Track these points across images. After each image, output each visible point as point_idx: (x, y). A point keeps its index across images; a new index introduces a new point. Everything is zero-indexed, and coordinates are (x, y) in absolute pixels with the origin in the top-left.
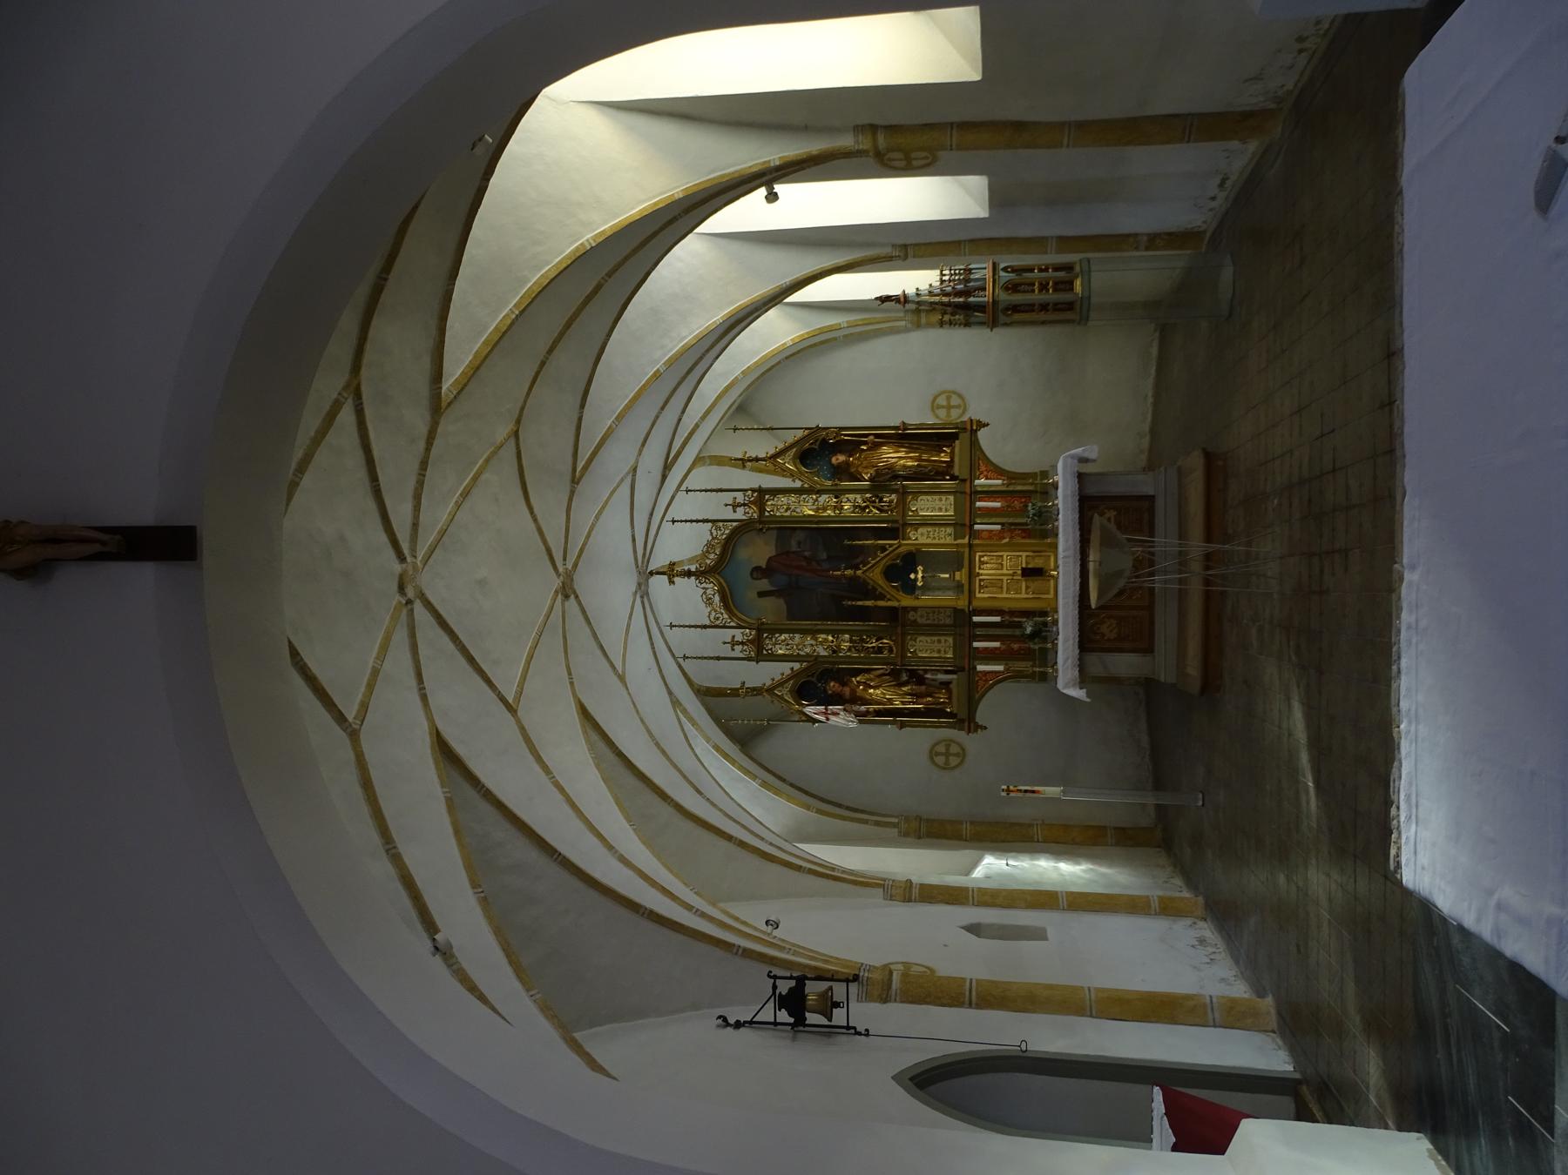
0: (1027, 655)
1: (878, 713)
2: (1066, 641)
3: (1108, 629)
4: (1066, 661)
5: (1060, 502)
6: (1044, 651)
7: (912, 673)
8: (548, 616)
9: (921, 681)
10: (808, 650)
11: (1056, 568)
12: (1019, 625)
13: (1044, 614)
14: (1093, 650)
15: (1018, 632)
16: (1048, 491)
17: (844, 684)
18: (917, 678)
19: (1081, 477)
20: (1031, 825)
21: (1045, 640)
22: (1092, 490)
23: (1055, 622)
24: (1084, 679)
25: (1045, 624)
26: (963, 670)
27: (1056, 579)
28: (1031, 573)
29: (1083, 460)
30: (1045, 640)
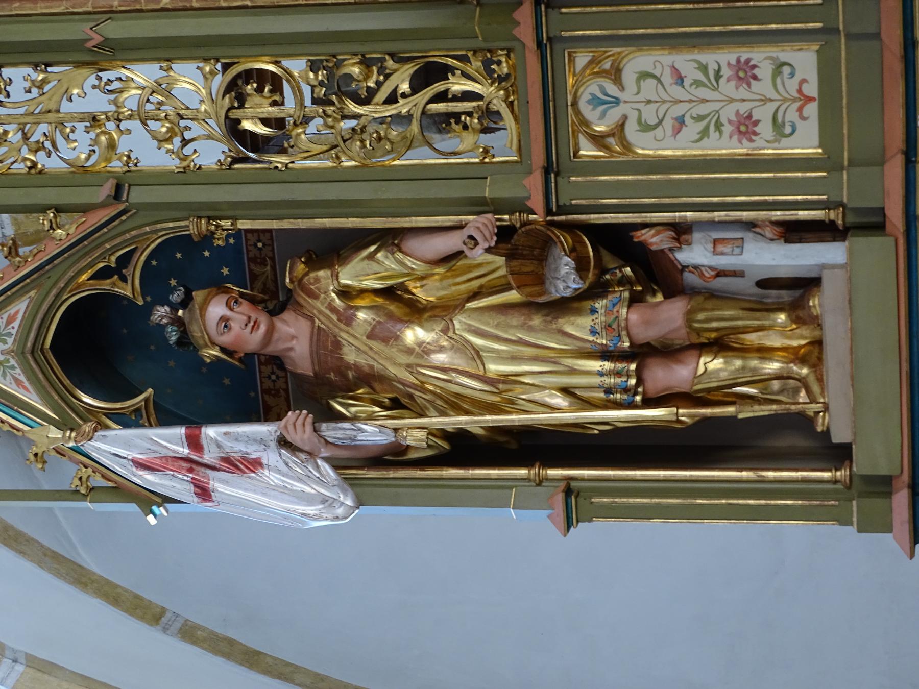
1: (461, 449)
7: (616, 241)
8: (89, 13)
9: (656, 275)
10: (78, 147)
17: (276, 300)
18: (629, 260)
26: (872, 224)
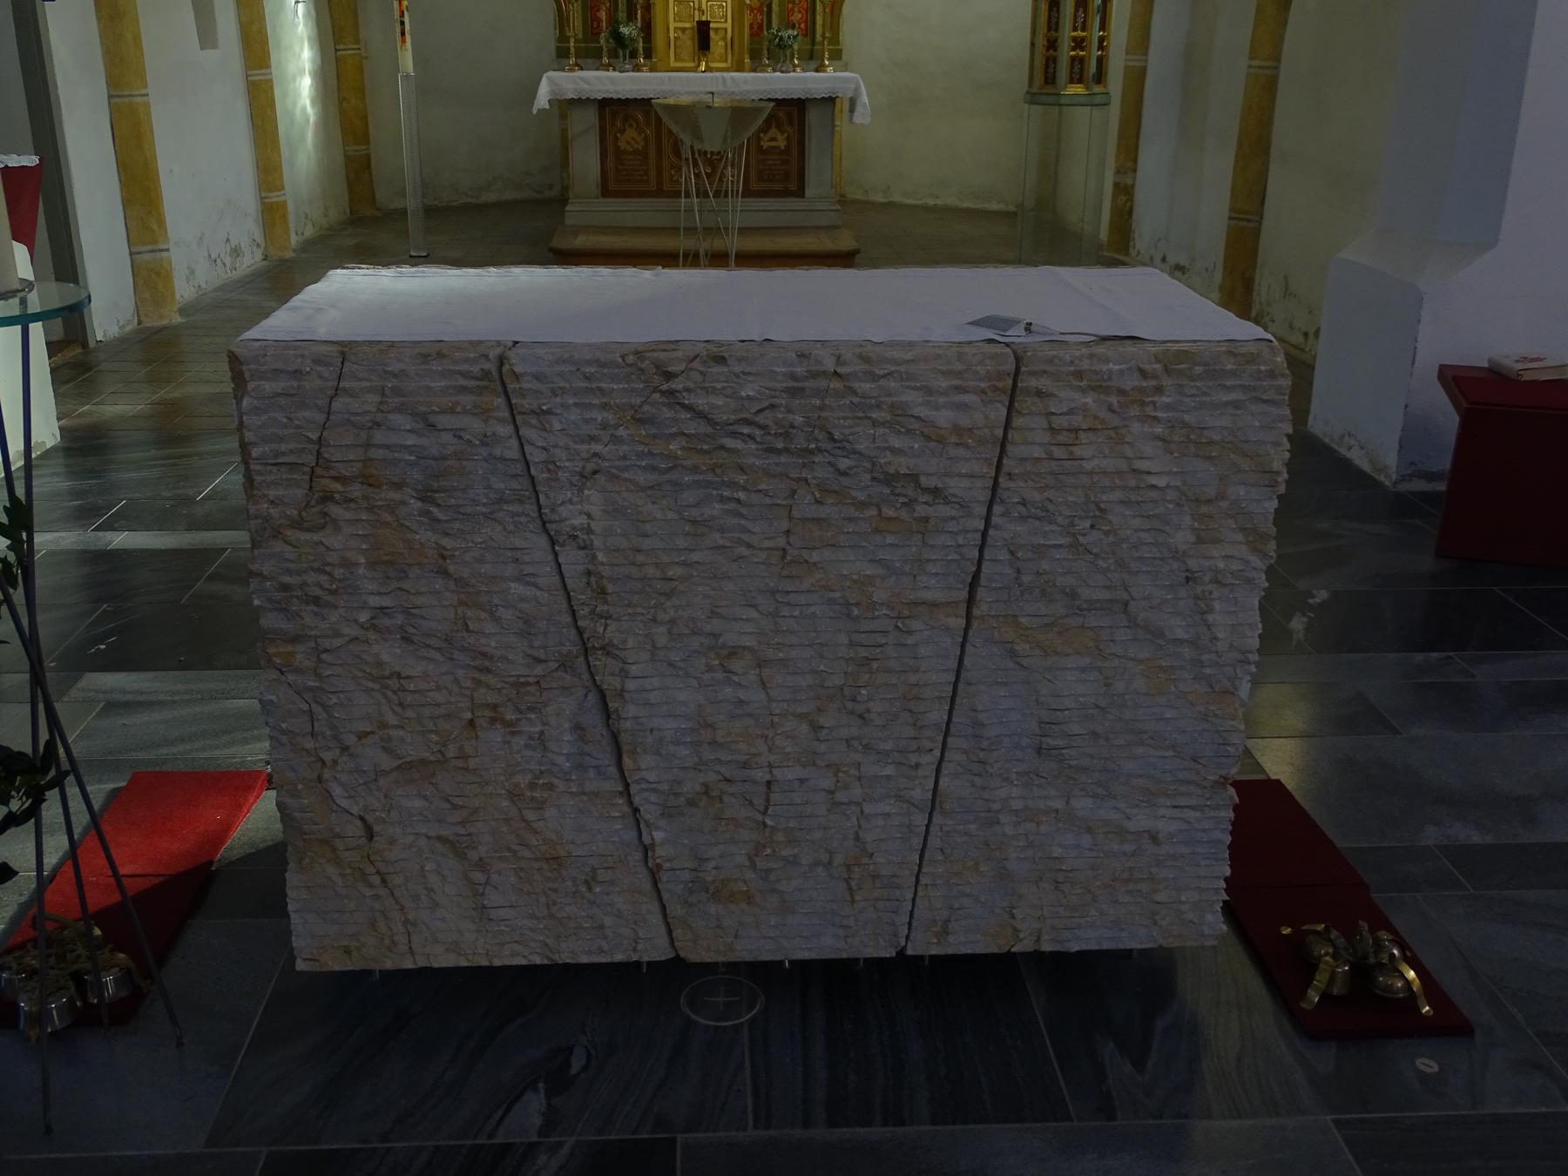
0: (592, 31)
2: (611, 80)
3: (630, 138)
4: (586, 81)
5: (799, 73)
6: (597, 54)
11: (709, 69)
12: (631, 17)
13: (648, 54)
14: (602, 117)
15: (622, 15)
16: (813, 58)
19: (830, 101)
20: (357, 41)
21: (613, 55)
22: (813, 116)
23: (637, 68)
24: (565, 106)
25: (634, 55)
27: (695, 70)
28: (703, 30)
29: (853, 102)
30: (613, 55)
